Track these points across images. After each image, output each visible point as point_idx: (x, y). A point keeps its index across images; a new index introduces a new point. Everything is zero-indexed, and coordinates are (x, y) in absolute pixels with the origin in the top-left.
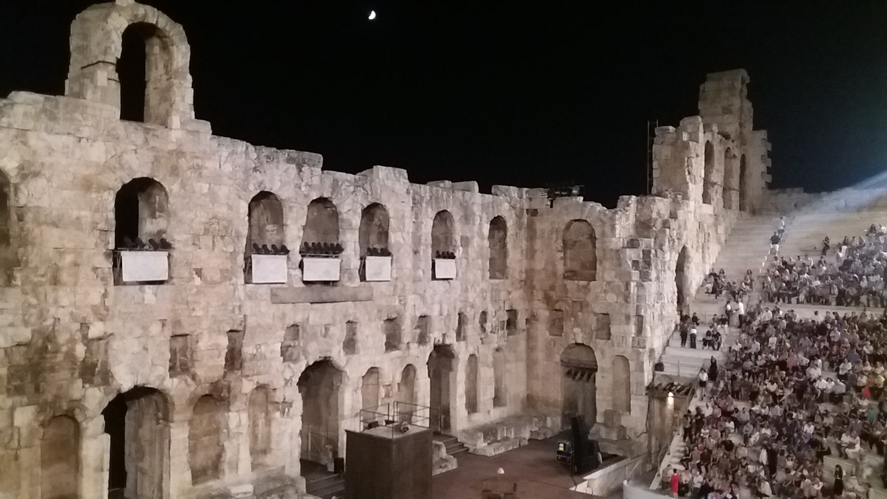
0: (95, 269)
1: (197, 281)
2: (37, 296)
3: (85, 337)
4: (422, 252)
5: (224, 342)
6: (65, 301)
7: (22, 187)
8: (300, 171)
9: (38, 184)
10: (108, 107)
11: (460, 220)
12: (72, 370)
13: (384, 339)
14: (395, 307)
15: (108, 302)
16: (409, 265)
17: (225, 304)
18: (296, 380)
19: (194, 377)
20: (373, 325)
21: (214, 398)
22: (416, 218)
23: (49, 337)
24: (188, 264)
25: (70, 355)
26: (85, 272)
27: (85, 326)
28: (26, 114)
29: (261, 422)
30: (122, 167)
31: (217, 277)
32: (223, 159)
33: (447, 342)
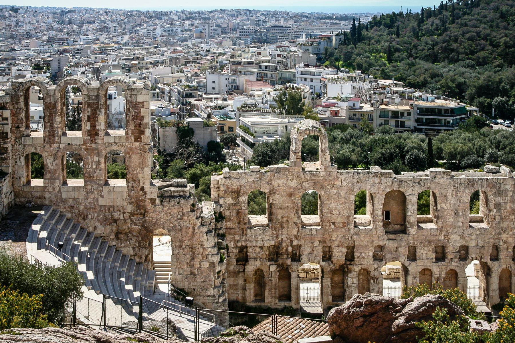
0: (294, 223)
1: (333, 227)
2: (276, 231)
3: (291, 245)
4: (461, 214)
5: (345, 250)
6: (285, 233)
7: (270, 197)
8: (381, 181)
10: (296, 168)
11: (495, 194)
12: (288, 255)
13: (434, 255)
14: (441, 240)
15: (299, 234)
16: (451, 220)
17: (344, 236)
19: (332, 262)
20: (426, 248)
23: (280, 244)
24: (329, 221)
25: (287, 250)
26: (291, 224)
27: (291, 241)
30: (302, 188)
31: (341, 225)
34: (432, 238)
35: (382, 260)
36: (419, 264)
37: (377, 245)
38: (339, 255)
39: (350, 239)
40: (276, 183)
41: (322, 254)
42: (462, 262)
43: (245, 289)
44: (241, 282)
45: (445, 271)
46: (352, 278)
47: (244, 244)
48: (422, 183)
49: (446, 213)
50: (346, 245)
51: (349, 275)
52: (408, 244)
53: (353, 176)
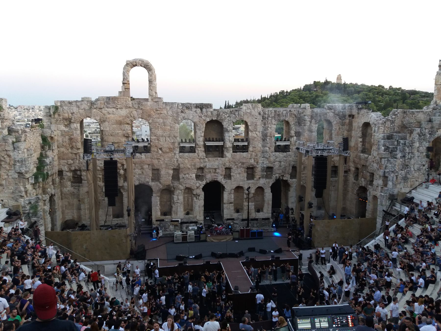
1: (160, 152)
4: (268, 140)
5: (171, 172)
8: (202, 110)
9: (106, 123)
13: (245, 175)
14: (251, 163)
18: (201, 187)
20: (239, 170)
21: (168, 191)
22: (265, 124)
28: (101, 103)
29: (190, 200)
31: (168, 150)
32: (168, 110)
33: (284, 179)
34: (244, 161)
35: (204, 180)
36: (233, 183)
37: (199, 167)
38: (166, 176)
39: (175, 162)
40: (106, 112)
41: (151, 175)
42: (267, 180)
43: (79, 209)
44: (75, 201)
45: (255, 188)
46: (178, 196)
47: (77, 168)
48: (237, 113)
49: (256, 139)
50: (172, 168)
51: (175, 194)
52: (224, 165)
53: (178, 106)
